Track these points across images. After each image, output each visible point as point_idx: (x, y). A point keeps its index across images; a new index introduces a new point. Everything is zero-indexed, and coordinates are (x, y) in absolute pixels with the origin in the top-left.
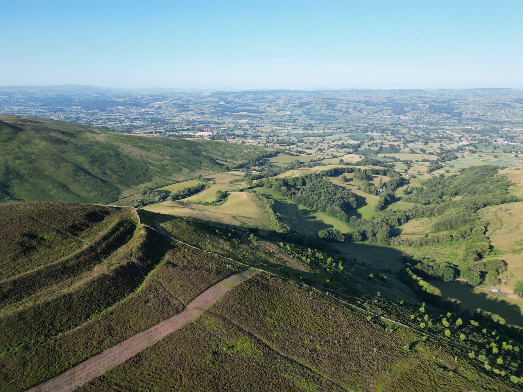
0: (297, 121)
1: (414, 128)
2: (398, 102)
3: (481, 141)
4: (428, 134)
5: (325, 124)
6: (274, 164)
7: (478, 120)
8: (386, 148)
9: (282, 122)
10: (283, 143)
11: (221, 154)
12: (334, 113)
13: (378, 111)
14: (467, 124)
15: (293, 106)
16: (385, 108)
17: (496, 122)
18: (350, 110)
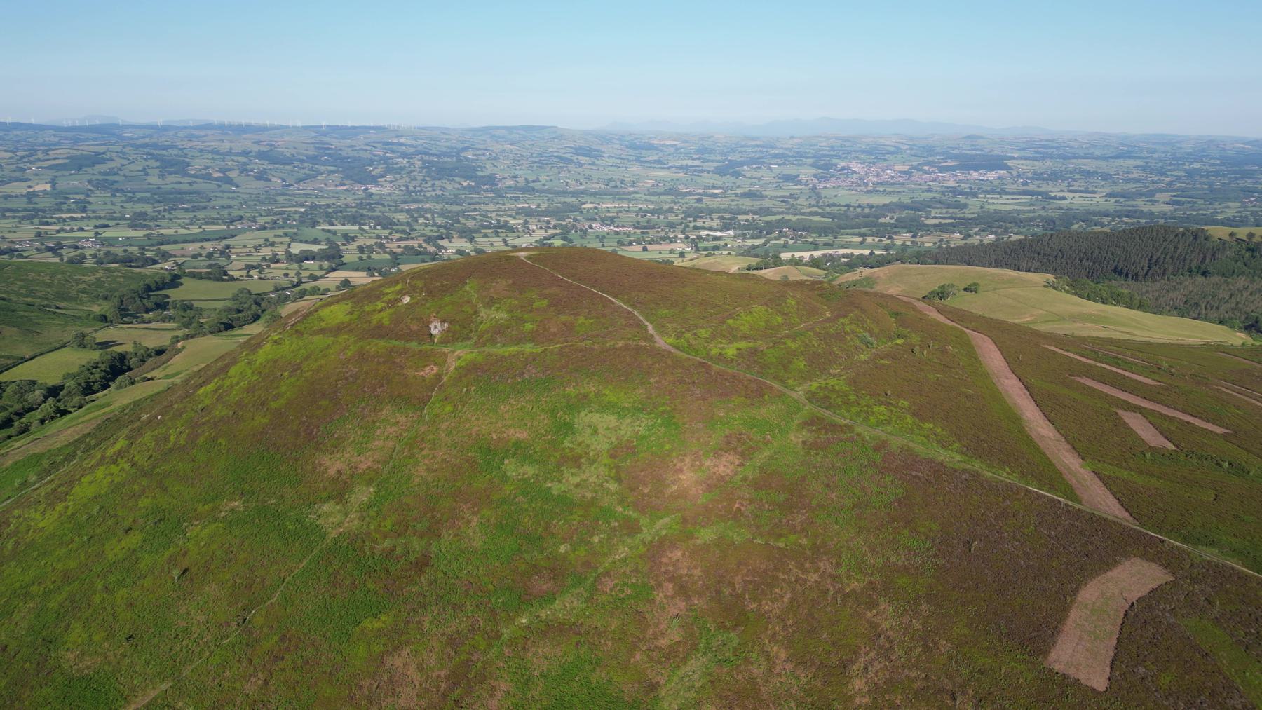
0: (90, 207)
1: (418, 210)
2: (344, 154)
3: (566, 229)
4: (459, 222)
5: (186, 210)
6: (196, 305)
7: (528, 189)
8: (403, 254)
9: (43, 211)
10: (128, 261)
11: (23, 291)
12: (191, 184)
13: (306, 178)
14: (517, 199)
15: (51, 167)
16: (322, 168)
17: (565, 193)
18: (230, 174)
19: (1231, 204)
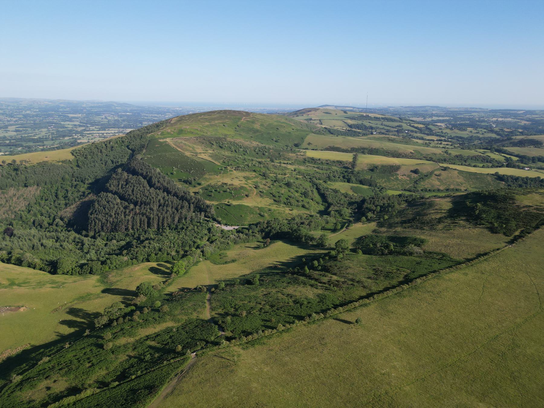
19: (43, 130)
